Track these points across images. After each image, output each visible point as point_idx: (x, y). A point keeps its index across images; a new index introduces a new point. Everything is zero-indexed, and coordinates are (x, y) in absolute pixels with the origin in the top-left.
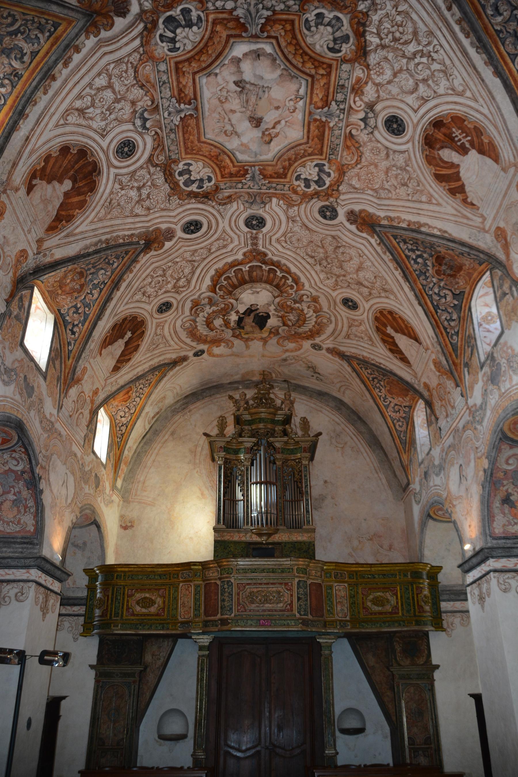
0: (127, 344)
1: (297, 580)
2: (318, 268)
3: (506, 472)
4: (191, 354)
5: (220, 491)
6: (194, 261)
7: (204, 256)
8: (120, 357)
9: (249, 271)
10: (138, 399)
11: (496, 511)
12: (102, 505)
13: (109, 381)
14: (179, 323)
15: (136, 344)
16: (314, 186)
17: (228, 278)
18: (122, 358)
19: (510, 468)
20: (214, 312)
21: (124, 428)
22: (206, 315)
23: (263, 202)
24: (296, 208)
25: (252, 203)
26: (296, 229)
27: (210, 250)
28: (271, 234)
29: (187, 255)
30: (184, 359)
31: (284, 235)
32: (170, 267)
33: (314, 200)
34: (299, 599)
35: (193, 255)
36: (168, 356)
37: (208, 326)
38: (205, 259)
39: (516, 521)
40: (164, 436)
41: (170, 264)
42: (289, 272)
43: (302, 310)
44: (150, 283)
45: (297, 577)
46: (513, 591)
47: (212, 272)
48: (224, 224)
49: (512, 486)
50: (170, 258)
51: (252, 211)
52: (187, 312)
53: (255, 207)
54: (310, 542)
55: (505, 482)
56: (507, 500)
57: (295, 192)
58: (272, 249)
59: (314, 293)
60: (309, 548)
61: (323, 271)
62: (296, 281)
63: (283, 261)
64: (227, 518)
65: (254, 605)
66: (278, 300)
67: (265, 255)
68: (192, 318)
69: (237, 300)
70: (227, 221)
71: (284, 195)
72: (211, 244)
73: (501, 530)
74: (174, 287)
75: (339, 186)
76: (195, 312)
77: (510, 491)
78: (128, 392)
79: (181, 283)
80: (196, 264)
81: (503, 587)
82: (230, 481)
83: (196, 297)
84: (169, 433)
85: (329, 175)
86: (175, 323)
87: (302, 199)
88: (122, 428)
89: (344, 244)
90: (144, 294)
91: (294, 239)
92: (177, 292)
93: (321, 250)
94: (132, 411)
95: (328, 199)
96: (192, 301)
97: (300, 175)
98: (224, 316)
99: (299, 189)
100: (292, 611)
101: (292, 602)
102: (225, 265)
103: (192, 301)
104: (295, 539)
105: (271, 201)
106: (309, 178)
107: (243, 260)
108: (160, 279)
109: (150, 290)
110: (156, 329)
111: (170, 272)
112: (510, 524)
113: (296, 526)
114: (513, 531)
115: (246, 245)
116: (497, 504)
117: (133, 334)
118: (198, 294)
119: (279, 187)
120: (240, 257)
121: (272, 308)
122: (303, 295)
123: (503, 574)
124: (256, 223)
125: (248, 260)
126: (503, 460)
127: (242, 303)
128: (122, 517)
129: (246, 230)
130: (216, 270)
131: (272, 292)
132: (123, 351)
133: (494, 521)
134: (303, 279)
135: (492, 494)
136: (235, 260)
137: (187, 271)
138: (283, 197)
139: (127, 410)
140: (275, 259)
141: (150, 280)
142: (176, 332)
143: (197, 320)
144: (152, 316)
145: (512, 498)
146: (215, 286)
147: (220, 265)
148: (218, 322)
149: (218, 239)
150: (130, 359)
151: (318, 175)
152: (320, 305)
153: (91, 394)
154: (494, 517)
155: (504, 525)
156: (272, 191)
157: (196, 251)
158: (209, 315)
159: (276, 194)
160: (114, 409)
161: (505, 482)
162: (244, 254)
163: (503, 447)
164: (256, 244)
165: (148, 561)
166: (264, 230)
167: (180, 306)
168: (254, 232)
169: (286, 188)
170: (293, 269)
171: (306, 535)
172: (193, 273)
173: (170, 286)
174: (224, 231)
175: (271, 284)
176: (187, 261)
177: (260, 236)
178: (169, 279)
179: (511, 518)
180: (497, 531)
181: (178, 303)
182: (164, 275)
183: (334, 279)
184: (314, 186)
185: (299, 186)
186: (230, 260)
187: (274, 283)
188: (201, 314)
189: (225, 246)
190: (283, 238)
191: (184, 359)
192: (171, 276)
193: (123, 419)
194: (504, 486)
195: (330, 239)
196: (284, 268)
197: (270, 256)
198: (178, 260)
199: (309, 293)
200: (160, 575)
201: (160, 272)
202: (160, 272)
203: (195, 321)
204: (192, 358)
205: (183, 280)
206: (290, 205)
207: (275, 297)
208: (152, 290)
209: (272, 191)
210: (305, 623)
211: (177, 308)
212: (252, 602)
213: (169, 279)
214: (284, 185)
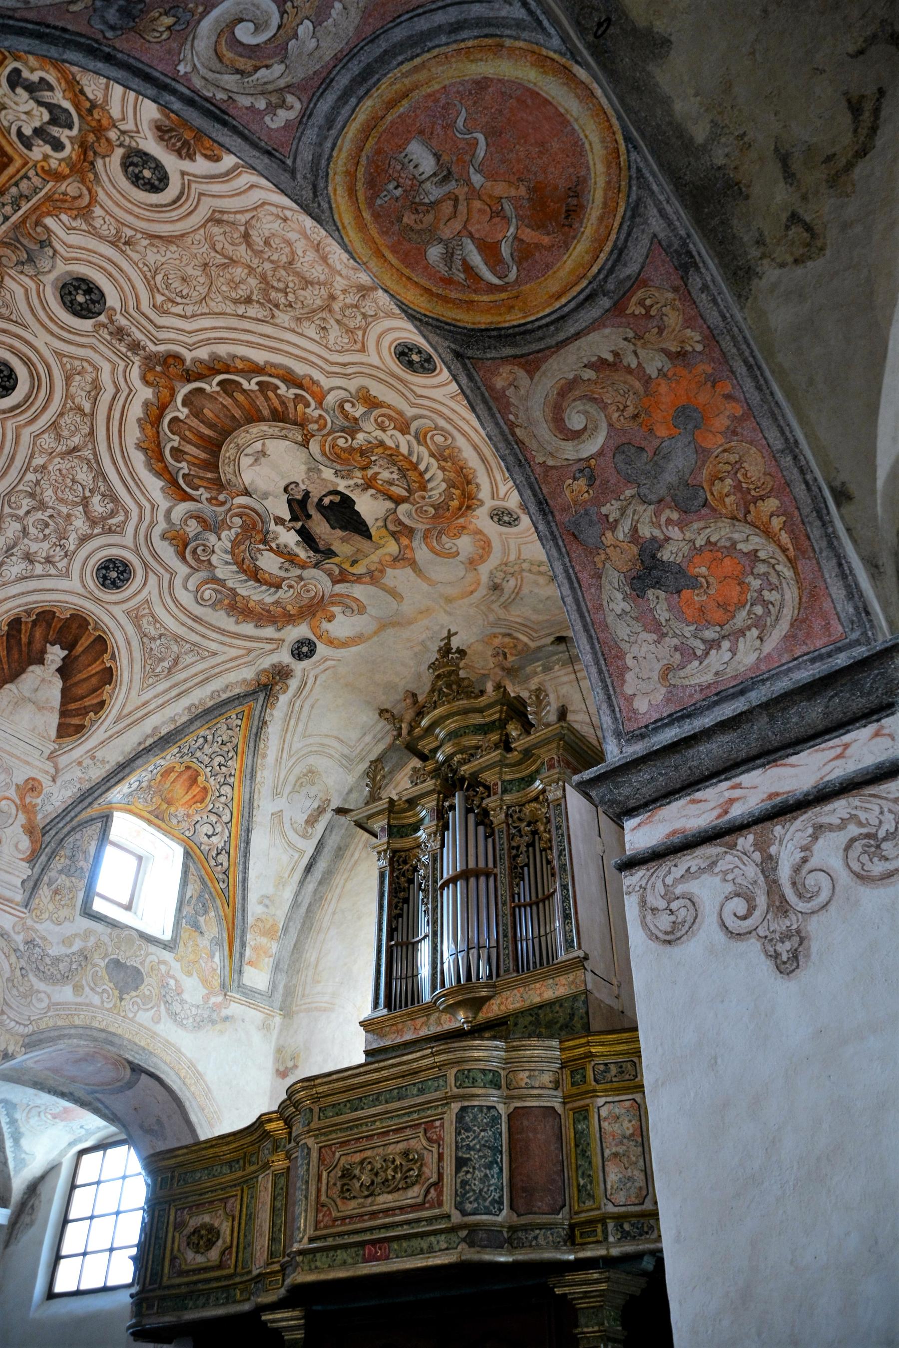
0: (64, 671)
1: (456, 1107)
2: (283, 318)
3: (587, 470)
4: (284, 657)
5: (380, 930)
6: (75, 449)
7: (86, 430)
8: (62, 704)
9: (197, 413)
10: (226, 790)
11: (622, 630)
12: (167, 1029)
13: (63, 761)
14: (186, 598)
15: (96, 668)
16: (63, 135)
17: (177, 453)
18: (73, 706)
19: (592, 446)
20: (235, 543)
21: (223, 858)
22: (228, 557)
23: (43, 244)
24: (98, 211)
25: (31, 260)
26: (152, 257)
27: (80, 409)
28: (131, 303)
29: (47, 441)
30: (281, 674)
31: (153, 289)
32: (38, 482)
33: (99, 163)
34: (461, 1163)
35: (59, 437)
36: (233, 677)
37: (258, 581)
38: (92, 433)
39: (710, 634)
40: (352, 855)
41: (30, 476)
42: (256, 369)
43: (382, 444)
44: (25, 531)
45: (455, 1098)
46: (709, 930)
47: (138, 459)
48: (41, 340)
49: (646, 513)
50: (18, 463)
51: (52, 276)
52: (182, 570)
53: (44, 263)
54: (575, 997)
55: (611, 509)
56: (650, 571)
57: (58, 177)
58: (172, 336)
59: (352, 385)
60: (572, 1016)
61: (299, 320)
62: (291, 380)
63: (222, 350)
64: (395, 990)
65: (353, 1204)
66: (314, 447)
67: (178, 358)
68: (202, 575)
69: (247, 493)
70: (36, 327)
71: (49, 198)
72: (68, 396)
73: (659, 695)
74: (93, 522)
75: (82, 92)
76: (198, 560)
77: (646, 531)
78: (194, 781)
79: (98, 506)
80: (87, 453)
81: (664, 921)
82: (406, 901)
83: (162, 526)
84: (361, 846)
85: (44, 84)
86: (175, 600)
87: (83, 181)
88: (223, 858)
89: (242, 218)
90: (29, 558)
91: (176, 285)
92: (110, 531)
93: (239, 272)
94: (226, 818)
95: (108, 140)
96: (163, 537)
97: (20, 133)
98: (265, 541)
99: (54, 164)
100: (440, 1204)
101: (440, 1176)
102: (142, 429)
103: (163, 537)
104: (537, 1000)
105: (46, 227)
106: (37, 124)
107: (157, 394)
108: (39, 515)
109: (41, 549)
110: (138, 627)
111: (49, 493)
112: (687, 653)
113: (544, 963)
114: (709, 678)
115: (123, 357)
116: (616, 602)
117: (69, 646)
118: (161, 518)
119: (24, 185)
120: (146, 393)
121: (328, 474)
122: (341, 407)
123: (668, 863)
124: (82, 298)
125: (166, 392)
126: (544, 431)
127: (265, 495)
128: (279, 1050)
129: (87, 325)
130: (138, 447)
131: (285, 437)
132: (64, 692)
133: (623, 670)
134: (300, 369)
135: (584, 576)
136: (146, 404)
137: (84, 476)
138: (55, 204)
139: (213, 818)
140: (203, 353)
141: (17, 526)
142: (197, 619)
143: (219, 574)
144: (97, 600)
145: (666, 555)
146: (174, 483)
147: (133, 434)
148: (269, 563)
149: (68, 379)
150: (102, 704)
151: (40, 103)
152: (389, 407)
153: (12, 793)
154: (621, 656)
155: (667, 671)
156: (25, 207)
157: (54, 426)
158: (233, 554)
159: (35, 208)
160: (185, 825)
161: (611, 509)
162: (147, 383)
163: (499, 383)
164: (135, 347)
165: (217, 1133)
166: (112, 299)
167: (150, 559)
168: (102, 318)
169: (37, 181)
170: (259, 357)
171: (562, 980)
172: (101, 474)
173: (80, 524)
174: (58, 354)
175: (261, 419)
176: (64, 455)
177: (123, 322)
178: (64, 510)
179: (688, 630)
180: (641, 705)
181: (137, 551)
182: (42, 506)
183: (332, 321)
184: (63, 135)
185: (46, 157)
186: (136, 411)
187: (266, 412)
188: (214, 559)
189: (96, 387)
190: (159, 299)
191: (281, 674)
192: (61, 500)
193: (213, 839)
194: (613, 526)
195: (216, 230)
196: (240, 365)
197: (188, 356)
198: (39, 461)
199: (343, 394)
200: (230, 1164)
201: (26, 503)
202: (26, 503)
203: (215, 580)
204: (299, 667)
205: (96, 499)
206: (85, 213)
207: (305, 444)
208: (46, 545)
209: (25, 207)
210: (473, 1235)
211: (146, 565)
212: (346, 1193)
213: (64, 510)
214: (26, 177)
